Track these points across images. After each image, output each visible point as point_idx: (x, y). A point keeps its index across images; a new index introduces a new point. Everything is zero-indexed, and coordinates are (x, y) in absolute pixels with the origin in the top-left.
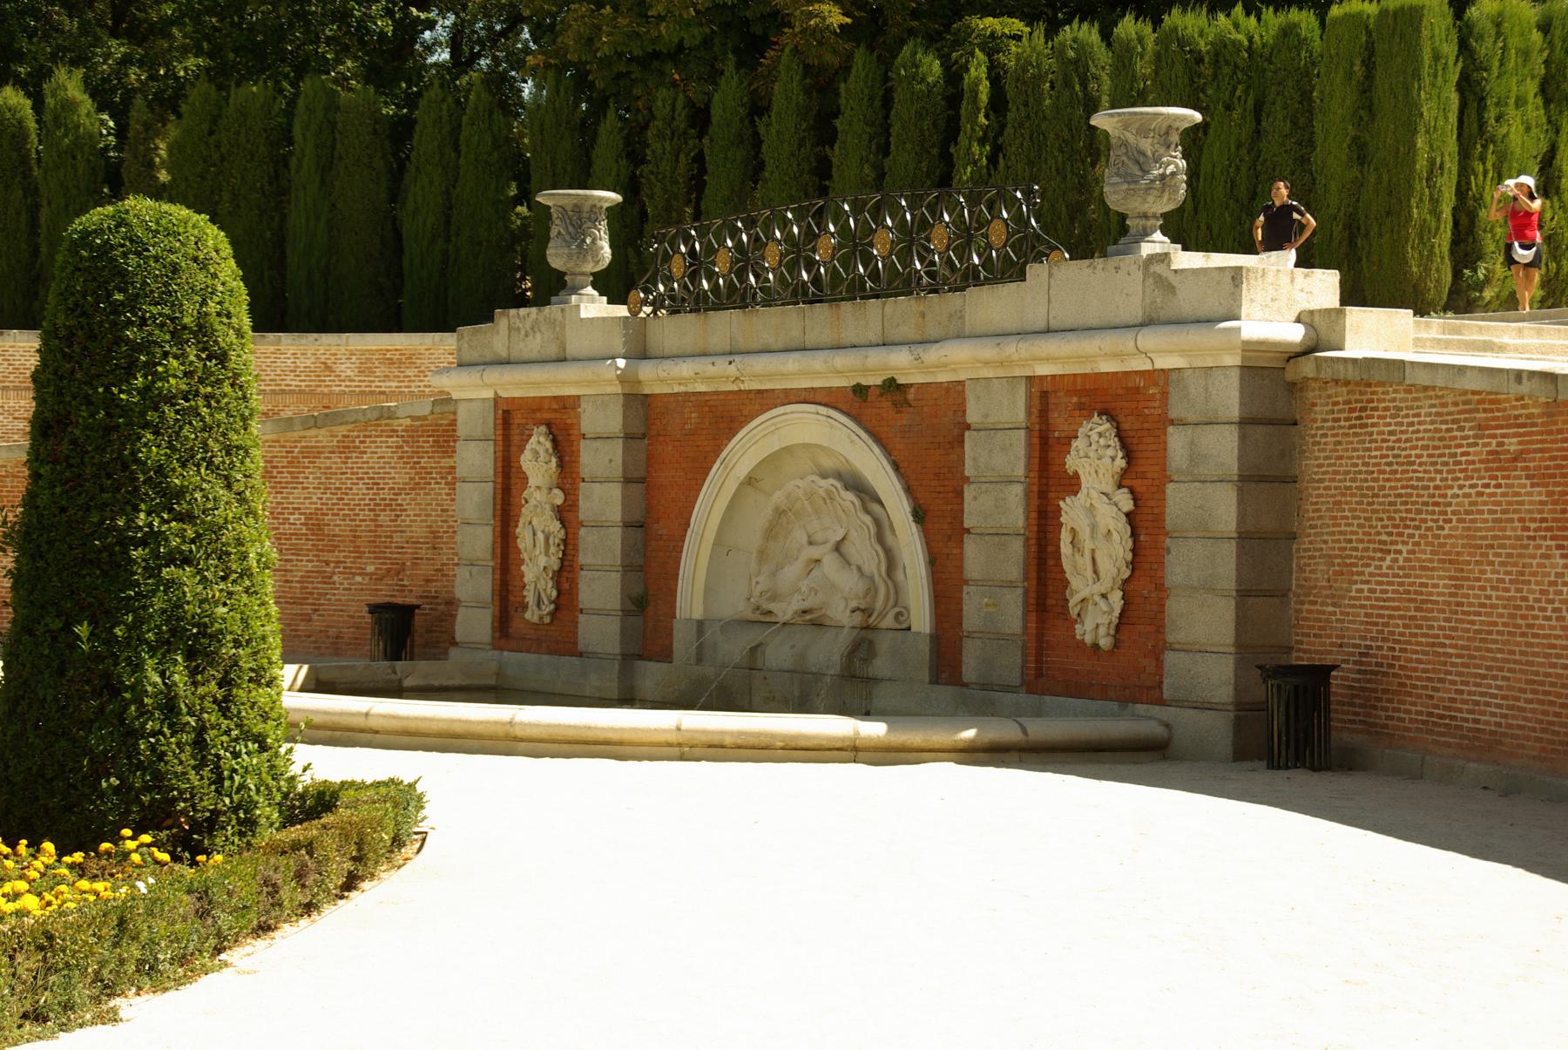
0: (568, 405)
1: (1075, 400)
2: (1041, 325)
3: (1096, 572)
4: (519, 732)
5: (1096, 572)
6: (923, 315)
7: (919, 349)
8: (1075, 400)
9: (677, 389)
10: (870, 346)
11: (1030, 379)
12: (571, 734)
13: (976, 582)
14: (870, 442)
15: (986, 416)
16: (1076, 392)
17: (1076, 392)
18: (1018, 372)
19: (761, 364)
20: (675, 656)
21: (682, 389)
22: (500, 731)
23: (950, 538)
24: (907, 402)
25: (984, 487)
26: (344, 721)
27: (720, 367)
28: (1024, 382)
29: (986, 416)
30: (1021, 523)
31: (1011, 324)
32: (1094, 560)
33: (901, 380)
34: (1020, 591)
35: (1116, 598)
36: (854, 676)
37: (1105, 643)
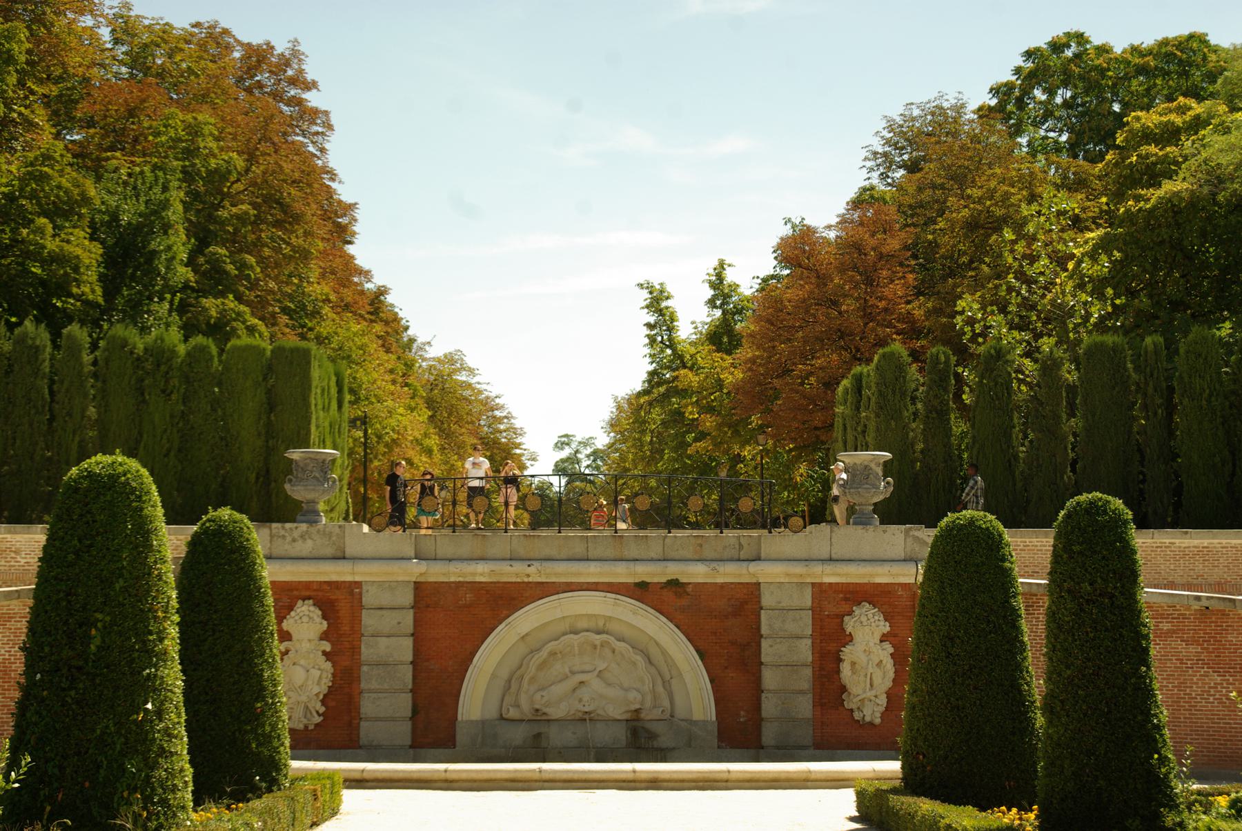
0: (353, 589)
1: (841, 596)
2: (827, 556)
3: (871, 685)
4: (813, 776)
5: (871, 685)
6: (701, 546)
7: (714, 565)
8: (841, 596)
9: (452, 579)
10: (652, 560)
11: (813, 584)
12: (836, 776)
13: (769, 691)
14: (657, 614)
15: (780, 603)
16: (841, 592)
17: (841, 592)
18: (809, 580)
19: (561, 567)
20: (458, 744)
21: (461, 579)
22: (804, 776)
23: (726, 668)
24: (685, 592)
25: (778, 640)
26: (712, 776)
27: (519, 567)
28: (810, 586)
29: (780, 603)
30: (810, 659)
31: (798, 555)
32: (871, 679)
33: (683, 580)
34: (810, 696)
35: (883, 700)
36: (639, 748)
37: (878, 721)
